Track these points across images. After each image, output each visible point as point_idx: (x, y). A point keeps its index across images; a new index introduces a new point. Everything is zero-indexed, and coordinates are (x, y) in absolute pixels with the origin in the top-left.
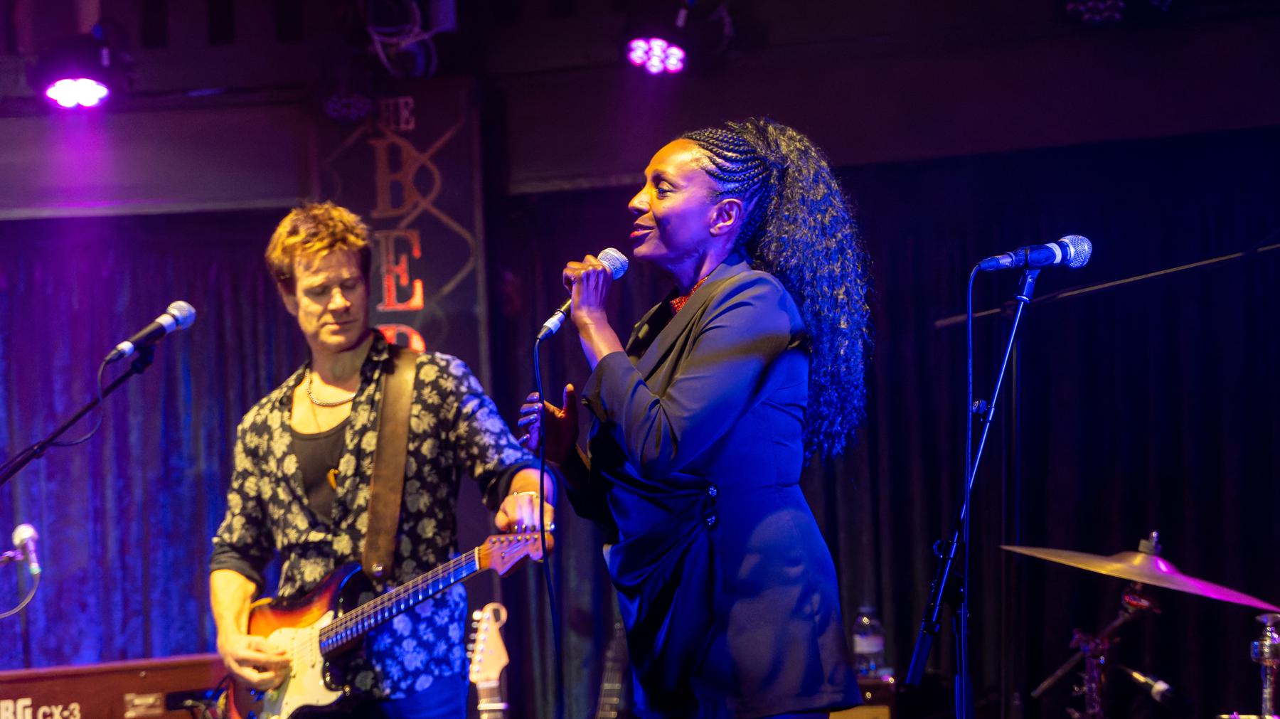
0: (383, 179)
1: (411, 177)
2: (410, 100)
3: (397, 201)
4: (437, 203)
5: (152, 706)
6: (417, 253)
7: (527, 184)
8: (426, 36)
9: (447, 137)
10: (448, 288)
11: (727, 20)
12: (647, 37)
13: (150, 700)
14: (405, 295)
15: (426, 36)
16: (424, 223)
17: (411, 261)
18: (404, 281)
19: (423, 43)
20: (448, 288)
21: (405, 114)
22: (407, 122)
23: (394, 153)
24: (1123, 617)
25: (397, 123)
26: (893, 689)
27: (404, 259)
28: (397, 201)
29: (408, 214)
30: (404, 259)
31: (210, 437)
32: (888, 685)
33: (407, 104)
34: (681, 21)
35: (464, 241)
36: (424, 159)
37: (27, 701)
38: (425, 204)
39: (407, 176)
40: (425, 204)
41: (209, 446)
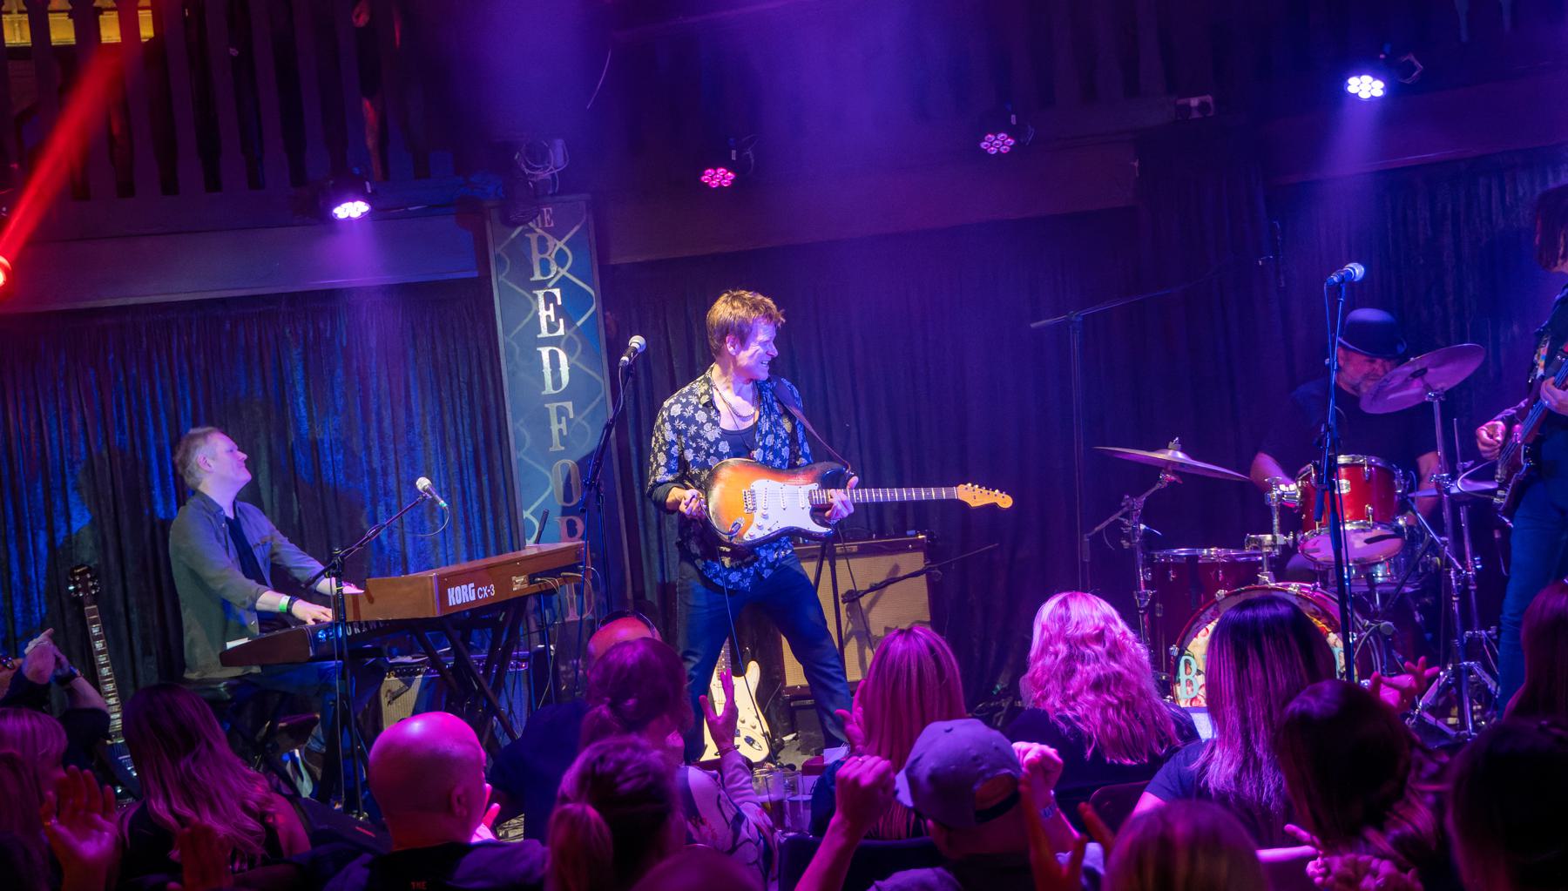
0: (536, 257)
1: (553, 255)
2: (550, 209)
3: (545, 270)
4: (568, 271)
5: (523, 583)
6: (559, 302)
7: (618, 259)
8: (555, 171)
10: (579, 324)
11: (751, 157)
12: (715, 167)
13: (520, 579)
15: (555, 171)
16: (563, 283)
17: (556, 307)
18: (553, 319)
19: (553, 175)
20: (579, 324)
21: (547, 217)
22: (549, 224)
23: (542, 242)
24: (1158, 486)
25: (543, 221)
26: (926, 541)
27: (551, 305)
28: (545, 271)
29: (553, 278)
30: (551, 305)
31: (433, 419)
33: (548, 211)
34: (734, 158)
35: (591, 296)
36: (560, 244)
37: (472, 585)
38: (563, 272)
39: (551, 256)
40: (563, 272)
41: (433, 428)
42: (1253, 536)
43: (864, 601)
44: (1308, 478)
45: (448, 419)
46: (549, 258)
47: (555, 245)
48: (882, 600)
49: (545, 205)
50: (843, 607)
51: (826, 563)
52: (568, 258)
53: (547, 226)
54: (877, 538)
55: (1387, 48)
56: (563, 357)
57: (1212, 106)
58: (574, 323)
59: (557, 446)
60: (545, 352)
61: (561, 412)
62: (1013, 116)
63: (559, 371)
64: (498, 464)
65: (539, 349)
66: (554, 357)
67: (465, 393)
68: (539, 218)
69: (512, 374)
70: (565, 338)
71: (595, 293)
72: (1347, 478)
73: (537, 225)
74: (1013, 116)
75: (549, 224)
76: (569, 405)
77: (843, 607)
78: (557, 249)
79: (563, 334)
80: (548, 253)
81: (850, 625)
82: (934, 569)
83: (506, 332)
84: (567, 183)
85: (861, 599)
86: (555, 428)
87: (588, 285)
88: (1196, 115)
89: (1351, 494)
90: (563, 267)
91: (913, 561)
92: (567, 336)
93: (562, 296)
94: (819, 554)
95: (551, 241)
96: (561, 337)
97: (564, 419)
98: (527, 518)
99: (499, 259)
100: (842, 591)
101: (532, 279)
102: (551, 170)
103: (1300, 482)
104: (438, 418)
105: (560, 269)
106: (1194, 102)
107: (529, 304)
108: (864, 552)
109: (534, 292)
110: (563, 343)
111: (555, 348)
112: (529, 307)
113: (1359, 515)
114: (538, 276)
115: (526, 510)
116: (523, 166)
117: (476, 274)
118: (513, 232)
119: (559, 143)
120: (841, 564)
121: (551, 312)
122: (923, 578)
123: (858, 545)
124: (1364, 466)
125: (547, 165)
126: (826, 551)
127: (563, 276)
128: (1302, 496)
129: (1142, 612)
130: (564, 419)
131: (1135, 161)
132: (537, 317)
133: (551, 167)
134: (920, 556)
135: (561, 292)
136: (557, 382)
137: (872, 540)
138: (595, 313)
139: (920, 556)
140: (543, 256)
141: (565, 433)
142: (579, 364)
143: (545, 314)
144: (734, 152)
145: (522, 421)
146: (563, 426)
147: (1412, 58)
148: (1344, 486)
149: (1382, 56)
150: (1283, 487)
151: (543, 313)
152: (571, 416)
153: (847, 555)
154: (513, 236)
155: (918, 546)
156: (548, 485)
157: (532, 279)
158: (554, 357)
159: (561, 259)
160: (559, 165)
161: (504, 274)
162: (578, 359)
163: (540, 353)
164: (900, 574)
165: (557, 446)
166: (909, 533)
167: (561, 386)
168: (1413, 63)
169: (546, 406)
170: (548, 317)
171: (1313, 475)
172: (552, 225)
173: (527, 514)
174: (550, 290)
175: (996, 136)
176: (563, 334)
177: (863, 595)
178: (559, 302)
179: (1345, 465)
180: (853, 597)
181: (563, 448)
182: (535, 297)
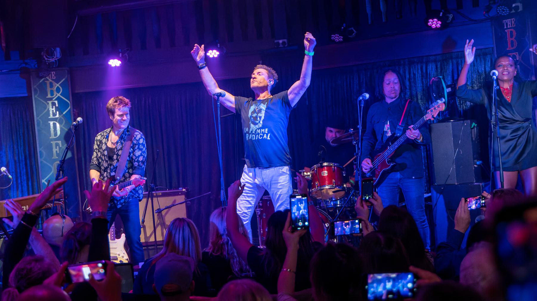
0: (49, 89)
1: (55, 89)
2: (54, 72)
3: (52, 94)
4: (61, 95)
6: (57, 106)
7: (79, 91)
8: (56, 59)
9: (62, 81)
10: (64, 113)
11: (127, 56)
12: (114, 59)
14: (54, 115)
15: (56, 59)
16: (58, 99)
17: (56, 107)
18: (55, 112)
19: (56, 60)
20: (64, 113)
21: (53, 75)
22: (54, 77)
23: (51, 84)
25: (52, 77)
27: (54, 107)
29: (55, 97)
30: (54, 107)
32: (185, 191)
33: (53, 73)
35: (68, 103)
36: (58, 85)
38: (59, 95)
40: (59, 95)
42: (295, 190)
43: (163, 213)
44: (314, 170)
45: (15, 147)
46: (53, 90)
47: (56, 85)
48: (170, 212)
49: (53, 71)
50: (156, 215)
51: (150, 199)
52: (60, 89)
53: (53, 78)
54: (168, 190)
55: (344, 25)
56: (58, 125)
57: (286, 43)
58: (62, 113)
59: (55, 157)
60: (51, 123)
61: (57, 145)
62: (219, 44)
63: (56, 130)
64: (33, 163)
65: (49, 122)
66: (55, 125)
67: (22, 138)
68: (50, 75)
69: (39, 131)
70: (58, 119)
71: (70, 103)
72: (327, 170)
73: (49, 78)
74: (219, 44)
75: (54, 77)
76: (60, 142)
77: (156, 215)
78: (56, 87)
79: (58, 116)
80: (53, 88)
81: (159, 221)
82: (188, 201)
83: (37, 117)
84: (60, 63)
85: (162, 212)
86: (54, 150)
87: (68, 100)
88: (281, 46)
89: (328, 176)
90: (58, 93)
91: (181, 198)
92: (60, 117)
93: (58, 103)
94: (147, 196)
95: (54, 83)
96: (58, 118)
97: (58, 147)
98: (44, 183)
99: (35, 90)
100: (155, 209)
101: (47, 97)
102: (55, 59)
103: (311, 172)
104: (12, 146)
105: (57, 94)
106: (281, 41)
107: (46, 106)
108: (164, 195)
109: (48, 102)
110: (58, 121)
111: (55, 122)
112: (45, 108)
113: (330, 183)
114: (49, 96)
115: (43, 179)
116: (45, 57)
117: (26, 95)
118: (41, 80)
119: (58, 49)
120: (155, 199)
121: (54, 109)
122: (185, 203)
123: (162, 193)
124: (332, 166)
125: (53, 57)
126: (150, 195)
127: (59, 97)
128: (311, 177)
129: (258, 216)
130: (58, 147)
131: (260, 61)
132: (49, 111)
133: (55, 57)
134: (183, 197)
135: (58, 102)
136: (56, 134)
137: (166, 190)
138: (70, 109)
139: (183, 197)
140: (52, 89)
141: (58, 152)
142: (63, 128)
143: (52, 110)
144: (121, 54)
145: (42, 148)
146: (58, 149)
147: (353, 29)
148: (325, 173)
149: (343, 28)
150: (305, 173)
151: (51, 109)
152: (61, 146)
153: (157, 196)
154: (41, 81)
155: (182, 193)
156: (51, 171)
157: (47, 97)
158: (55, 125)
159: (58, 90)
160: (58, 57)
161: (37, 95)
162: (63, 126)
163: (50, 123)
164: (177, 203)
165: (55, 157)
166: (181, 188)
167: (56, 136)
168: (353, 30)
169: (51, 142)
170: (53, 111)
171: (316, 169)
172: (55, 78)
173: (43, 181)
174: (53, 101)
175: (212, 51)
176: (58, 116)
177: (163, 210)
178: (57, 106)
179: (326, 166)
180: (159, 211)
181: (57, 158)
182: (48, 103)
